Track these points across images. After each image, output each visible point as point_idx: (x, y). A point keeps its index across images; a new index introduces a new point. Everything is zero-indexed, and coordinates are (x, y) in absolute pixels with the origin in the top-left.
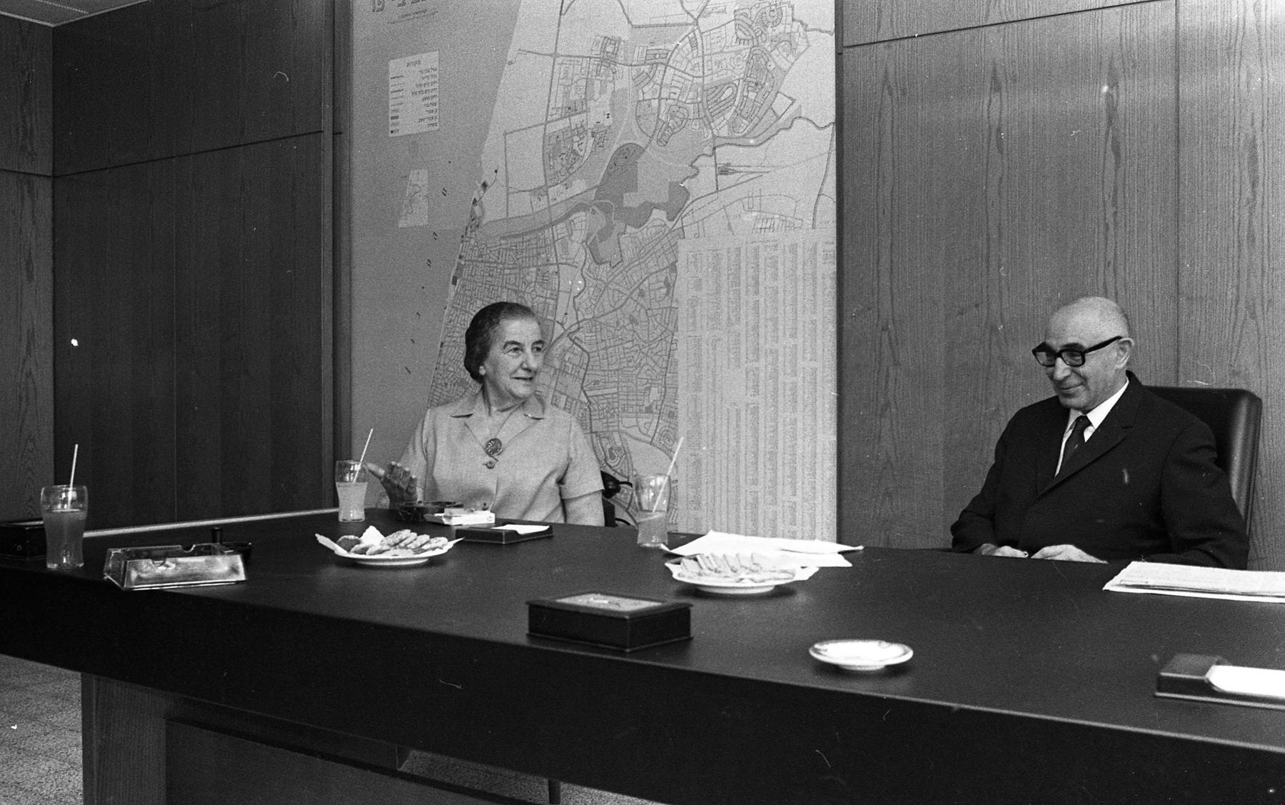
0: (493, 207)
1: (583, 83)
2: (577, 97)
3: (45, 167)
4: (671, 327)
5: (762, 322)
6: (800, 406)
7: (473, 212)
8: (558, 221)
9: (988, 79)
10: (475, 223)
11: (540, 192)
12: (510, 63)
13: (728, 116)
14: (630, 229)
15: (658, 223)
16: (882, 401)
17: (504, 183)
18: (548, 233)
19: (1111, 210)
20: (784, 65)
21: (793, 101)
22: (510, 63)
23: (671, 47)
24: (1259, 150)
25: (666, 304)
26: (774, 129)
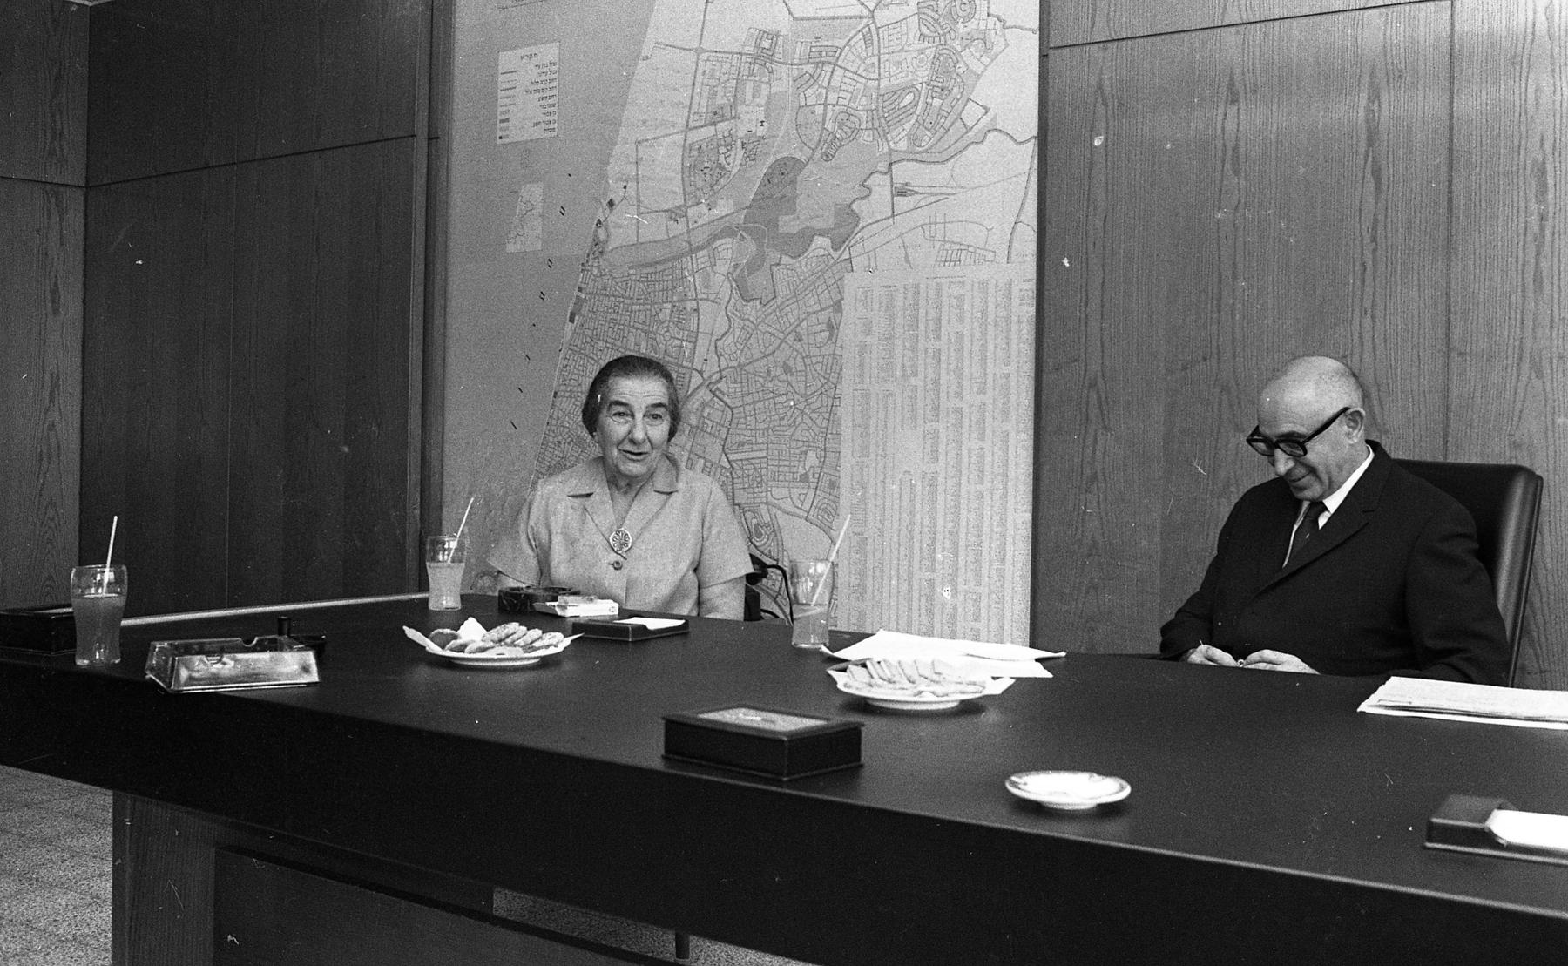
3: (75, 173)
6: (988, 478)
8: (699, 248)
9: (1224, 90)
10: (598, 247)
11: (674, 215)
12: (646, 58)
13: (907, 126)
14: (786, 259)
15: (822, 252)
16: (1088, 471)
20: (978, 68)
21: (987, 110)
22: (646, 58)
23: (841, 43)
24: (1550, 181)
26: (965, 141)
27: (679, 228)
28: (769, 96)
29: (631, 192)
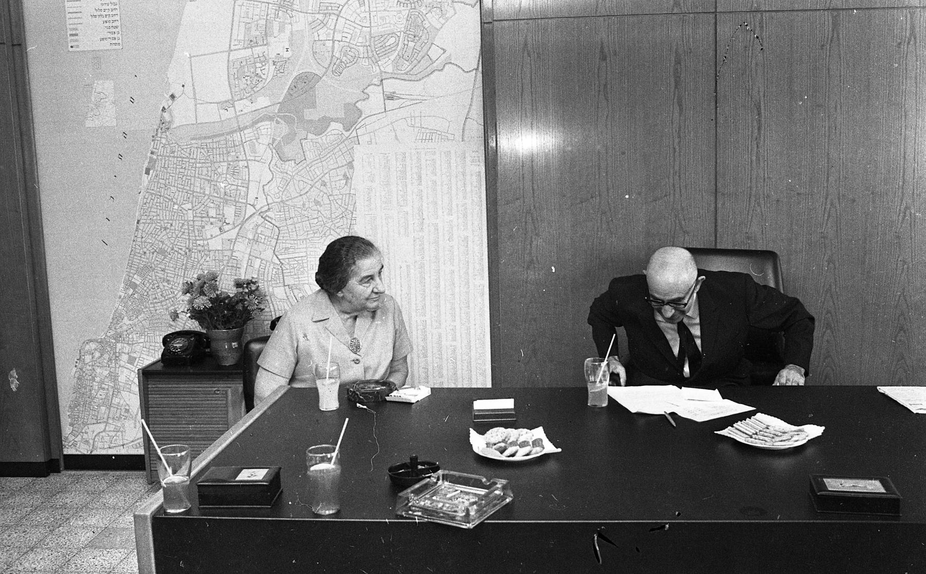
0: (182, 114)
1: (263, 22)
2: (258, 33)
4: (351, 208)
5: (425, 205)
7: (162, 116)
8: (246, 128)
9: (598, 51)
10: (164, 126)
11: (225, 105)
13: (392, 58)
14: (310, 136)
15: (336, 132)
17: (191, 95)
18: (237, 136)
19: (677, 141)
21: (445, 51)
25: (346, 190)
27: (226, 115)
28: (291, 33)
29: (188, 89)
